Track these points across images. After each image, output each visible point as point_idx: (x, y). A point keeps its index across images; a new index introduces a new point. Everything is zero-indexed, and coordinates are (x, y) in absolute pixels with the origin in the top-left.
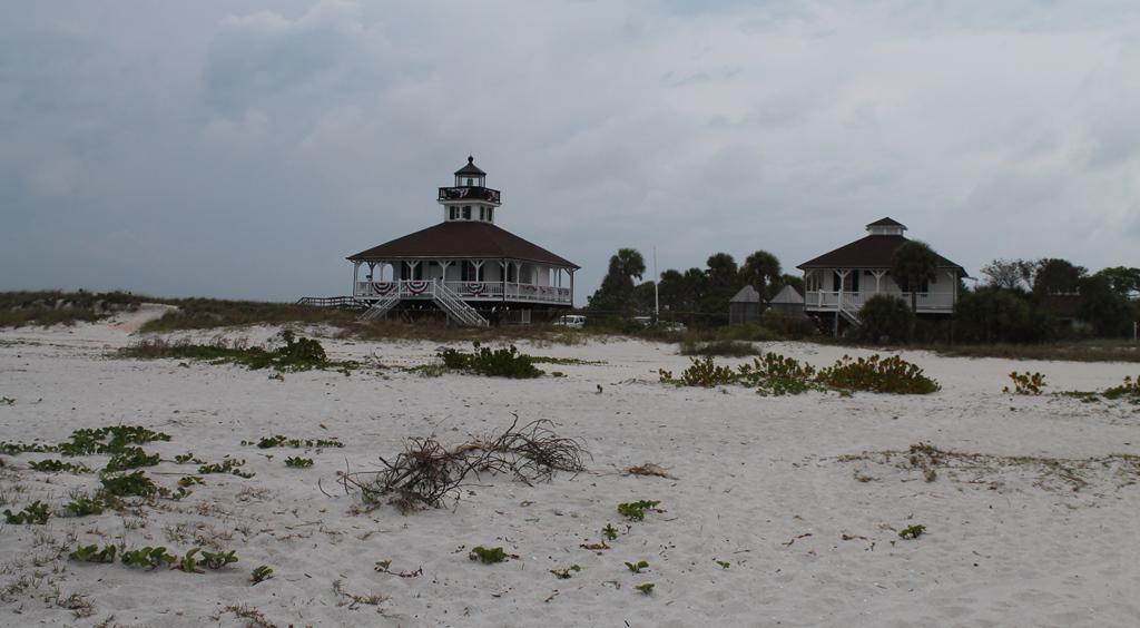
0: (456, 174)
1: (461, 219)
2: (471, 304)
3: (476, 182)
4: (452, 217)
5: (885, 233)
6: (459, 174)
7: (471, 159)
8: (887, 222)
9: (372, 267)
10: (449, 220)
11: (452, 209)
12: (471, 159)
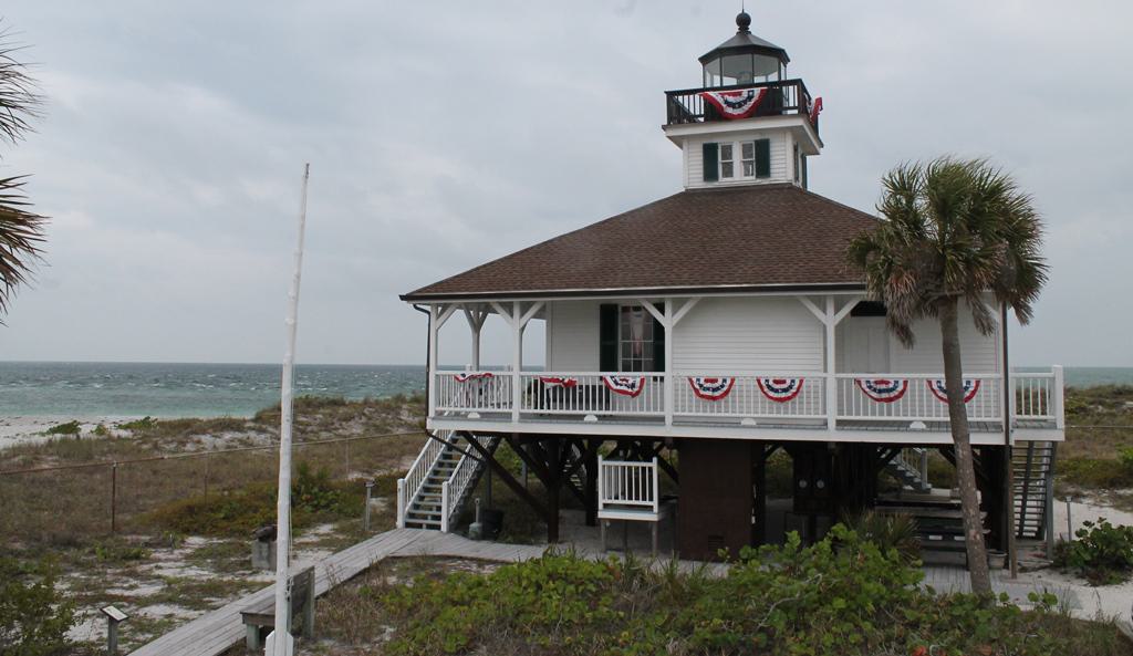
0: (705, 60)
4: (710, 174)
7: (744, 21)
9: (477, 326)
10: (698, 182)
11: (710, 152)
12: (744, 21)
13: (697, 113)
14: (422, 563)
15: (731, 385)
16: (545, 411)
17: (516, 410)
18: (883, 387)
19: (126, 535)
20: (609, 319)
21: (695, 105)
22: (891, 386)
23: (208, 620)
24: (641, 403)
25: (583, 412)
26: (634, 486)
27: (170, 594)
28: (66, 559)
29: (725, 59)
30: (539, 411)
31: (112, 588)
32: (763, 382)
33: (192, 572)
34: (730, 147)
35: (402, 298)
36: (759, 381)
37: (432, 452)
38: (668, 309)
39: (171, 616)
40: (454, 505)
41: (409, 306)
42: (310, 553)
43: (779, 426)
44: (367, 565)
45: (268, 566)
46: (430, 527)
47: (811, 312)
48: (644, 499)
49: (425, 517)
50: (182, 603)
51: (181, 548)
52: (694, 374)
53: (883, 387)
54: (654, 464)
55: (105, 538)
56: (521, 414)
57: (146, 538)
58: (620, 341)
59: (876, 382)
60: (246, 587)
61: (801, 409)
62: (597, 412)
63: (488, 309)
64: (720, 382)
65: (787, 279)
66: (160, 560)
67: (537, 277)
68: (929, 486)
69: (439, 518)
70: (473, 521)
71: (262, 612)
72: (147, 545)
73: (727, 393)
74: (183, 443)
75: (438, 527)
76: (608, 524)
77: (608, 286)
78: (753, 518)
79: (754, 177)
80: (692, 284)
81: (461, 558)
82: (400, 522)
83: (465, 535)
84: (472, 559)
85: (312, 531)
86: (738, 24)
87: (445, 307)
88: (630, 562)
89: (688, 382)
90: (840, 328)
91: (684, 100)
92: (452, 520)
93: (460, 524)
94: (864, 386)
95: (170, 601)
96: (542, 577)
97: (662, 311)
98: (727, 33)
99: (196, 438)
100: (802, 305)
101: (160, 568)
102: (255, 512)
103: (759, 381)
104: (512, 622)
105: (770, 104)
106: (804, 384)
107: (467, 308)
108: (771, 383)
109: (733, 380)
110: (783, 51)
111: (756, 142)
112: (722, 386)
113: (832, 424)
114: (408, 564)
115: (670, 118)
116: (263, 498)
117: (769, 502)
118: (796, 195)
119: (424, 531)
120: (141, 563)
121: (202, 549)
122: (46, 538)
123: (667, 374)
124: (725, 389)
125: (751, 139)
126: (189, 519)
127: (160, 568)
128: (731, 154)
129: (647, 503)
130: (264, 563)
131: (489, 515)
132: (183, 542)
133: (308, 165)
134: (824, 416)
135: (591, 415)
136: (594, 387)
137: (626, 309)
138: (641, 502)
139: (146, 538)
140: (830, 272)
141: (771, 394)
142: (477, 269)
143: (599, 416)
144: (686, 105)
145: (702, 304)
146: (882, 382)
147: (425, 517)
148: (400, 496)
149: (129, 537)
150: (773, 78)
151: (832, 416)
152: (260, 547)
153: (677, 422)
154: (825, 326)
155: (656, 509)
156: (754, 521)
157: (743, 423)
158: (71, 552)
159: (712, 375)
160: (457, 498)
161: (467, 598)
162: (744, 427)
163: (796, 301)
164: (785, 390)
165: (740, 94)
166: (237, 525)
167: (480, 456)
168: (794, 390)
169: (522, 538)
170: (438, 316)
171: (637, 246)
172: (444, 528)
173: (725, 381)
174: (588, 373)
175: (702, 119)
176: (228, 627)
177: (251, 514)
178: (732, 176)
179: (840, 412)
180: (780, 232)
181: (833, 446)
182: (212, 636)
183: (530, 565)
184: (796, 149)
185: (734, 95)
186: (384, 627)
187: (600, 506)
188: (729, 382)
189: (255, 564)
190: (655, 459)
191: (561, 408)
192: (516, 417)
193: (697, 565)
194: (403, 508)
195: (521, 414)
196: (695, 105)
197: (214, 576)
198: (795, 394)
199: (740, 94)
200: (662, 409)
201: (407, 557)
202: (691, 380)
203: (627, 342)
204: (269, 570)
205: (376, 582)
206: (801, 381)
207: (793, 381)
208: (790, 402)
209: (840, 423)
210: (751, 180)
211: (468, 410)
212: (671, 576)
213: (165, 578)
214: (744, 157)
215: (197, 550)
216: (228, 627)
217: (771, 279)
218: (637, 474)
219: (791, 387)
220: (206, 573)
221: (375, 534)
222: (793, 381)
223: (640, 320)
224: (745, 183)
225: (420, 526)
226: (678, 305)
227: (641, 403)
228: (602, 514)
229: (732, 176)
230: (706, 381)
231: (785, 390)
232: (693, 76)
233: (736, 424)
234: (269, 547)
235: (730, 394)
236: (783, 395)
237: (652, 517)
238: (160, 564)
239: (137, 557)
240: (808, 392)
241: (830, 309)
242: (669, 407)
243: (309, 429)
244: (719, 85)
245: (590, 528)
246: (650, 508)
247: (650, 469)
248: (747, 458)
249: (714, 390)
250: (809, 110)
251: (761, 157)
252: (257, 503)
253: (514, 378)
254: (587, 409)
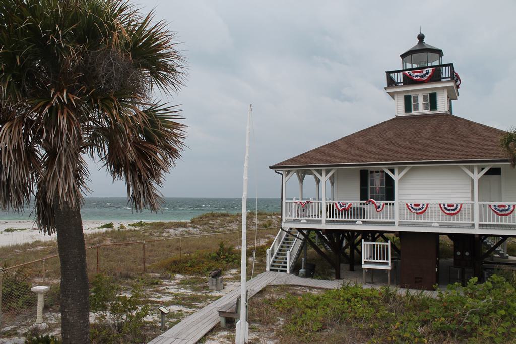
0: (403, 56)
1: (421, 110)
4: (408, 109)
7: (421, 38)
9: (301, 180)
10: (402, 113)
11: (408, 99)
12: (421, 38)
13: (399, 81)
14: (284, 288)
15: (427, 207)
16: (334, 219)
18: (503, 208)
19: (149, 273)
20: (364, 176)
21: (399, 78)
22: (507, 208)
23: (198, 315)
24: (383, 215)
25: (355, 219)
26: (377, 253)
27: (177, 301)
28: (128, 283)
29: (413, 55)
30: (331, 219)
31: (151, 297)
32: (442, 206)
33: (182, 291)
34: (417, 97)
35: (270, 167)
36: (440, 205)
37: (279, 239)
38: (396, 172)
39: (180, 311)
40: (292, 261)
41: (273, 171)
42: (231, 283)
43: (450, 226)
44: (261, 289)
45: (215, 289)
46: (281, 271)
47: (467, 175)
48: (384, 260)
49: (279, 267)
50: (184, 305)
51: (174, 280)
52: (409, 202)
53: (503, 208)
54: (389, 244)
55: (141, 274)
56: (326, 220)
57: (159, 275)
58: (370, 187)
59: (499, 206)
60: (209, 298)
61: (461, 218)
62: (362, 219)
63: (306, 172)
64: (421, 206)
65: (454, 158)
66: (167, 285)
67: (333, 158)
68: (507, 255)
69: (286, 267)
70: (302, 269)
71: (228, 311)
72: (160, 278)
73: (425, 210)
74: (162, 233)
75: (286, 271)
76: (367, 271)
77: (368, 163)
78: (437, 269)
79: (429, 110)
80: (408, 160)
81: (300, 286)
82: (267, 269)
83: (297, 274)
84: (306, 286)
85: (228, 273)
86: (419, 39)
87: (289, 172)
88: (387, 290)
89: (406, 206)
90: (479, 181)
91: (393, 75)
92: (291, 269)
93: (295, 270)
94: (493, 208)
95: (178, 304)
96: (349, 296)
97: (392, 171)
98: (414, 43)
99: (167, 230)
100: (462, 170)
101: (168, 288)
102: (202, 264)
103: (440, 205)
104: (340, 317)
105: (436, 76)
106: (463, 207)
107: (298, 172)
108: (446, 206)
109: (427, 205)
110: (441, 51)
111: (430, 94)
112: (423, 208)
113: (477, 226)
114: (278, 288)
116: (204, 258)
117: (442, 261)
118: (448, 117)
119: (279, 273)
120: (159, 286)
121: (183, 280)
122: (118, 274)
123: (396, 202)
124: (424, 209)
126: (176, 267)
127: (168, 288)
128: (418, 100)
129: (385, 261)
130: (214, 287)
131: (309, 266)
132: (174, 277)
133: (251, 105)
134: (473, 222)
135: (359, 221)
136: (357, 208)
137: (372, 172)
138: (382, 261)
139: (159, 275)
140: (475, 154)
141: (447, 211)
142: (304, 154)
143: (363, 221)
144: (393, 77)
145: (412, 169)
146: (502, 206)
147: (279, 267)
148: (268, 257)
149: (151, 274)
150: (436, 63)
151: (477, 222)
152: (212, 280)
153: (401, 224)
154: (472, 181)
155: (389, 264)
156: (437, 271)
157: (432, 225)
158: (129, 281)
159: (417, 202)
160: (293, 258)
161: (314, 305)
162: (433, 227)
163: (458, 167)
164: (453, 210)
165: (422, 71)
166: (195, 269)
167: (303, 238)
168: (458, 210)
169: (325, 276)
170: (287, 175)
171: (378, 143)
172: (288, 270)
173: (423, 205)
174: (355, 202)
175: (402, 84)
176: (210, 317)
177: (201, 264)
178: (418, 110)
179: (481, 220)
180: (446, 136)
181: (478, 236)
182: (205, 321)
183: (342, 290)
184: (448, 97)
185: (420, 72)
186: (278, 318)
187: (363, 263)
188: (425, 206)
189: (210, 287)
190: (389, 241)
191: (342, 218)
192: (323, 222)
193: (419, 292)
194: (269, 261)
195: (326, 220)
196: (399, 78)
197: (192, 293)
198: (458, 211)
199: (422, 71)
200: (393, 218)
201: (277, 285)
202: (407, 205)
203: (376, 186)
204: (217, 290)
205: (268, 297)
206: (461, 206)
207: (457, 205)
208: (455, 216)
209: (481, 226)
210: (428, 112)
211: (301, 218)
212: (407, 295)
213: (172, 293)
214: (424, 101)
215: (181, 280)
216: (210, 317)
217: (446, 158)
218: (377, 248)
219: (456, 208)
220: (189, 291)
221: (257, 274)
222: (457, 205)
223: (379, 177)
224: (426, 113)
225: (277, 271)
226: (401, 170)
227: (383, 215)
228: (364, 266)
229: (418, 110)
230: (415, 205)
231: (453, 210)
232: (398, 64)
233: (429, 225)
234: (217, 280)
235: (426, 211)
236: (452, 212)
237: (388, 268)
238: (168, 287)
239: (157, 283)
240: (465, 211)
241: (476, 171)
242: (396, 217)
243: (215, 226)
244: (411, 68)
245: (353, 272)
246: (387, 264)
247: (387, 246)
248: (426, 242)
249: (419, 209)
250: (455, 77)
251: (432, 101)
252: (202, 260)
253: (475, 205)
254: (358, 218)
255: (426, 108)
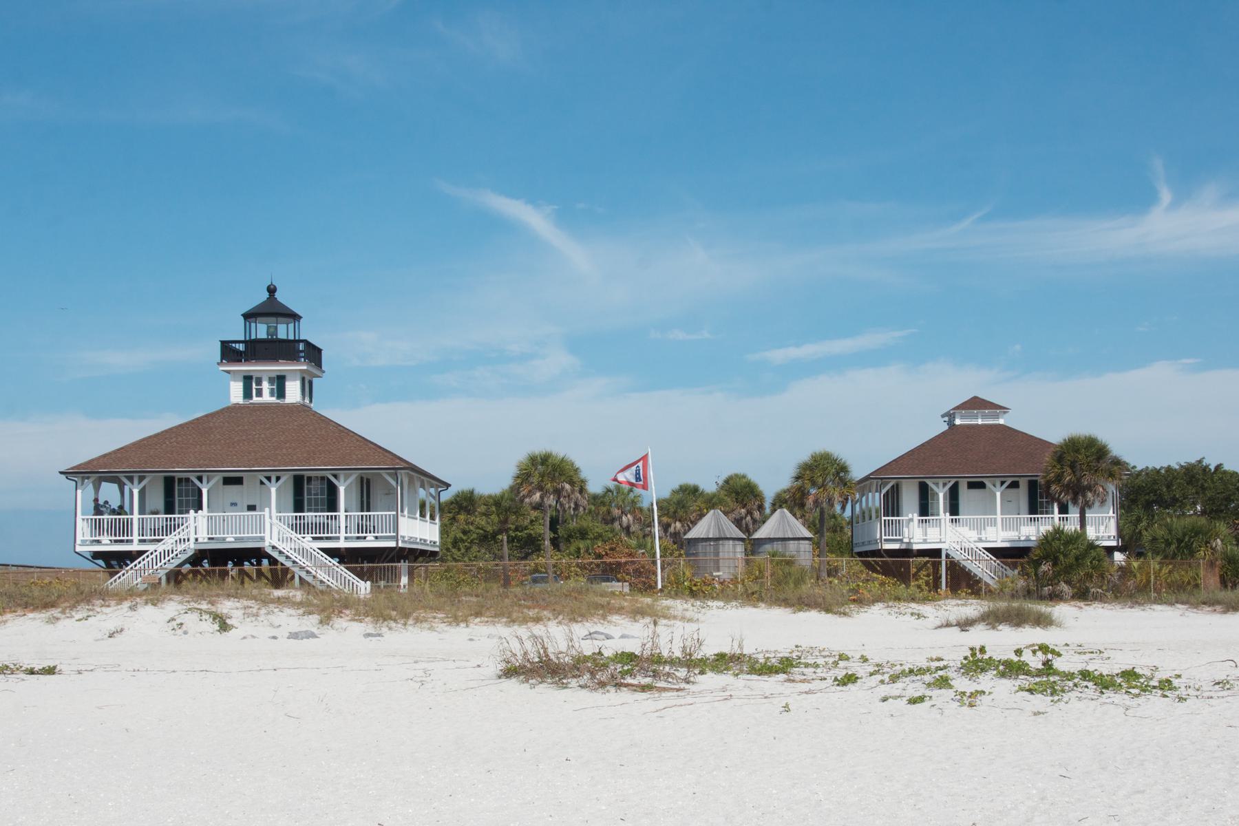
1: (267, 398)
2: (323, 550)
3: (284, 331)
4: (247, 394)
5: (980, 422)
6: (249, 316)
7: (272, 290)
8: (976, 404)
9: (97, 489)
12: (272, 290)
17: (136, 537)
41: (63, 477)
115: (223, 357)
125: (274, 375)
251: (279, 383)
255: (272, 394)
